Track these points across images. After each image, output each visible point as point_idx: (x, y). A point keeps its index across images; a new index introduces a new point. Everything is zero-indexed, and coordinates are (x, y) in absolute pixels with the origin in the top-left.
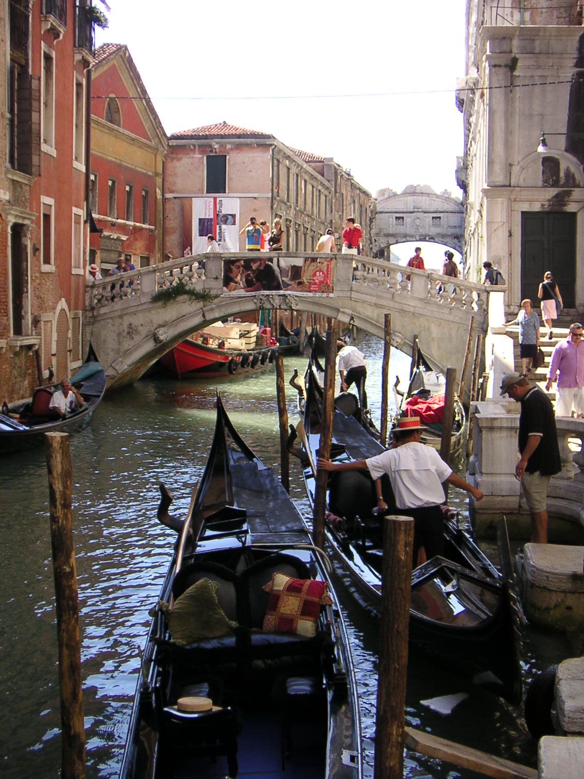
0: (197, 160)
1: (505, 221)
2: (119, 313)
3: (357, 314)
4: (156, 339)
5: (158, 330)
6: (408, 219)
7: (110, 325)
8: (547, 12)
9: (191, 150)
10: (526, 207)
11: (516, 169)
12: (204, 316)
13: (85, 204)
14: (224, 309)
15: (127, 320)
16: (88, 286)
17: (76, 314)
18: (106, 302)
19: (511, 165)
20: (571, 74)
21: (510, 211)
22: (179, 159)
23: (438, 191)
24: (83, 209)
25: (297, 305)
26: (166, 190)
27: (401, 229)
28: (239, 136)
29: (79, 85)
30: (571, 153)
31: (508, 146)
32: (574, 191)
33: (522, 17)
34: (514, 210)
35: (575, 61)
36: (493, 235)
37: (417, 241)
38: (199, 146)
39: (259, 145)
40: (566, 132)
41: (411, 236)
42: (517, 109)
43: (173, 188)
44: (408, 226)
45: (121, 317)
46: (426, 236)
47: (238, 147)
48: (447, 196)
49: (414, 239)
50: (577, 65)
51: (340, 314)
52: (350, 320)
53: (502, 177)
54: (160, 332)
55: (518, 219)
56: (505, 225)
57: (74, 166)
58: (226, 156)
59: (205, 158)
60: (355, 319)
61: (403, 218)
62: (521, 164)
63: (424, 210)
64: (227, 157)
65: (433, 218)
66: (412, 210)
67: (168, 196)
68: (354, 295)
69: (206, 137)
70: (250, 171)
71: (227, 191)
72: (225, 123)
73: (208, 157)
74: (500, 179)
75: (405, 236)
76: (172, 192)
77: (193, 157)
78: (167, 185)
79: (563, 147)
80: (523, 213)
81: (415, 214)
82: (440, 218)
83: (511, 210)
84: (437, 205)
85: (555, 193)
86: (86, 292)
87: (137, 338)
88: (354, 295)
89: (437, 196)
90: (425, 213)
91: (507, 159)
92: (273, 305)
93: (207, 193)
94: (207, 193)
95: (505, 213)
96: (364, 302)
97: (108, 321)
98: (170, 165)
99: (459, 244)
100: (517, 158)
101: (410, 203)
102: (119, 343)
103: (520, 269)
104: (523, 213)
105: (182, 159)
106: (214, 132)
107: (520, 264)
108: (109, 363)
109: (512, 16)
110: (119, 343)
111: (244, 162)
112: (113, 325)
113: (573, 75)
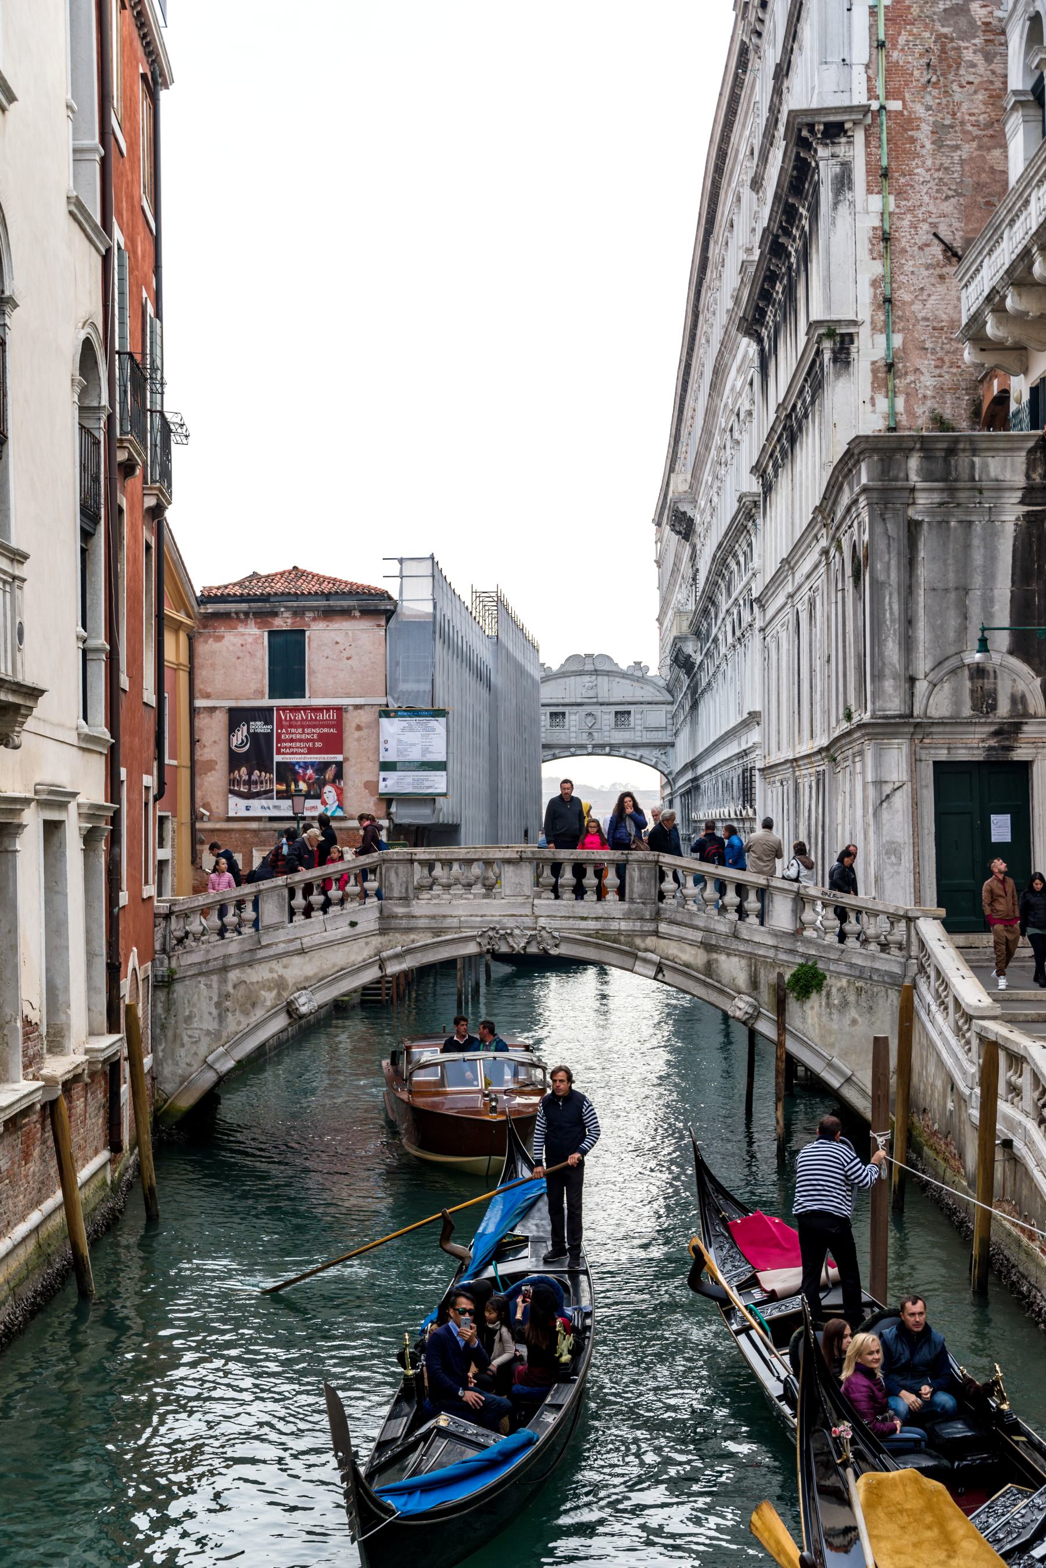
0: (250, 640)
1: (905, 779)
2: (218, 964)
3: (669, 963)
4: (290, 1010)
5: (296, 995)
6: (574, 719)
7: (202, 986)
8: (934, 397)
9: (241, 621)
10: (943, 755)
11: (921, 686)
12: (381, 968)
13: (155, 764)
14: (419, 955)
15: (233, 976)
16: (156, 916)
17: (146, 971)
18: (194, 944)
19: (912, 680)
20: (1013, 518)
21: (915, 761)
22: (219, 639)
23: (624, 663)
24: (152, 775)
25: (557, 946)
26: (197, 694)
27: (560, 736)
28: (328, 596)
29: (148, 547)
30: (1018, 657)
31: (908, 645)
32: (1026, 723)
33: (892, 406)
34: (921, 760)
35: (1019, 494)
36: (885, 805)
37: (589, 754)
38: (254, 613)
39: (367, 613)
40: (1006, 623)
41: (583, 747)
42: (922, 580)
43: (209, 690)
44: (573, 729)
45: (225, 969)
46: (603, 746)
47: (328, 614)
48: (639, 674)
49: (585, 752)
50: (1022, 502)
51: (637, 963)
52: (657, 973)
53: (897, 701)
54: (302, 1000)
55: (928, 773)
56: (905, 787)
57: (145, 700)
58: (304, 631)
59: (266, 634)
60: (665, 972)
61: (563, 714)
62: (930, 677)
63: (601, 700)
64: (307, 633)
65: (617, 713)
66: (579, 700)
67: (199, 703)
68: (663, 927)
69: (265, 598)
70: (348, 658)
71: (307, 694)
72: (295, 568)
73: (271, 633)
74: (894, 705)
75: (568, 747)
76: (208, 696)
77: (243, 635)
78: (199, 685)
79: (1005, 649)
80: (935, 763)
81: (584, 707)
82: (629, 713)
83: (916, 760)
84: (622, 691)
85: (992, 729)
86: (155, 926)
87: (259, 1014)
88: (663, 927)
89: (624, 675)
90: (602, 704)
91: (907, 668)
92: (512, 947)
93: (270, 698)
94: (270, 698)
95: (904, 765)
96: (681, 939)
97: (199, 979)
98: (203, 648)
99: (663, 758)
100: (922, 665)
101: (574, 689)
102: (221, 1018)
103: (934, 865)
104: (935, 763)
105: (223, 637)
106: (279, 587)
107: (934, 856)
108: (201, 1057)
109: (873, 405)
110: (221, 1018)
111: (337, 643)
112: (209, 986)
113: (1018, 519)
